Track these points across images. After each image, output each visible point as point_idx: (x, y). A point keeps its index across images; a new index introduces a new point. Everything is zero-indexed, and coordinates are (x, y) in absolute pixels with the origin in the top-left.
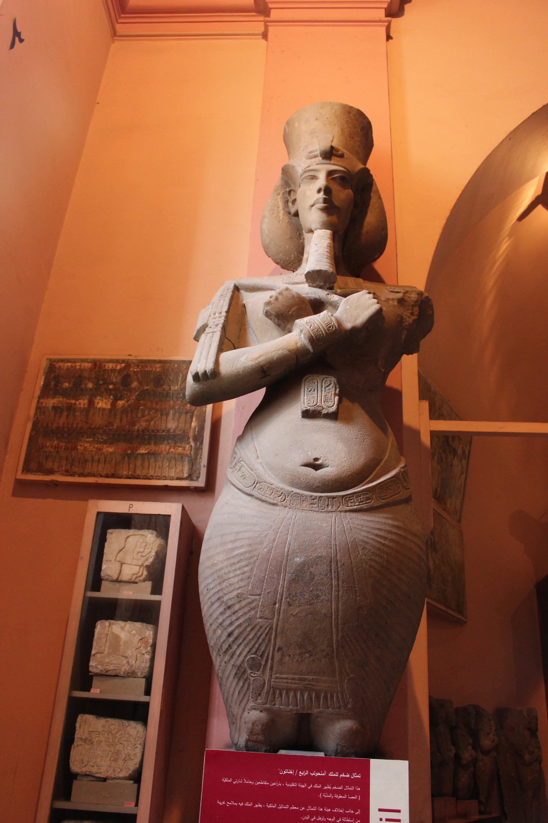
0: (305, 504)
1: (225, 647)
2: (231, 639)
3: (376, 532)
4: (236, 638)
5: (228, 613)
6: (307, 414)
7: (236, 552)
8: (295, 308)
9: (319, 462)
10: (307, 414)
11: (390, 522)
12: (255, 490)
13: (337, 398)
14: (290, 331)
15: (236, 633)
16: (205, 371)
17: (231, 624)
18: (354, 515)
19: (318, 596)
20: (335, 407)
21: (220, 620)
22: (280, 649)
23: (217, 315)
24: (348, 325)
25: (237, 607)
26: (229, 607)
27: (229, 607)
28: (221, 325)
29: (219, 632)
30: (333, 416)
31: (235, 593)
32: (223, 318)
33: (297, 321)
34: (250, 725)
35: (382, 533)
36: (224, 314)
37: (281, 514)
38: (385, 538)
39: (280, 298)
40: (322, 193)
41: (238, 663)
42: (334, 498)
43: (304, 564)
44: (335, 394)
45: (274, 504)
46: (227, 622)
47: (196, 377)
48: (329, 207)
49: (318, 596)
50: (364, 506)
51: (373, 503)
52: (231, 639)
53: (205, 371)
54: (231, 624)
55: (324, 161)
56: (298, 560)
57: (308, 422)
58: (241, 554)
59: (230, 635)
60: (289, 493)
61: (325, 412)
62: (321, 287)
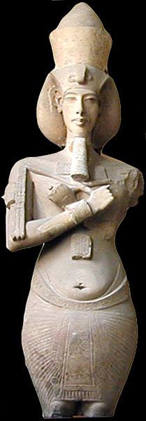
0: (76, 307)
1: (41, 373)
2: (43, 370)
3: (111, 319)
4: (46, 370)
5: (42, 358)
6: (74, 258)
7: (43, 331)
8: (65, 197)
9: (82, 285)
10: (74, 258)
11: (118, 313)
12: (50, 298)
13: (90, 248)
14: (64, 210)
15: (46, 368)
16: (20, 237)
17: (43, 363)
18: (100, 311)
19: (84, 350)
20: (89, 254)
21: (37, 361)
22: (67, 374)
23: (19, 194)
24: (96, 209)
25: (45, 356)
26: (42, 356)
27: (42, 356)
28: (23, 204)
29: (37, 367)
30: (90, 259)
31: (44, 350)
32: (23, 197)
33: (67, 206)
34: (54, 407)
35: (114, 320)
36: (23, 194)
37: (67, 313)
38: (115, 322)
39: (58, 191)
40: (79, 115)
41: (48, 380)
42: (89, 303)
43: (76, 336)
44: (89, 246)
45: (61, 307)
46: (41, 363)
47: (15, 239)
48: (84, 123)
49: (84, 350)
50: (104, 307)
51: (108, 305)
52: (43, 370)
53: (20, 237)
54: (43, 363)
55: (81, 86)
56: (74, 334)
57: (74, 261)
58: (47, 331)
59: (43, 368)
60: (68, 302)
61: (84, 257)
62: (80, 181)
